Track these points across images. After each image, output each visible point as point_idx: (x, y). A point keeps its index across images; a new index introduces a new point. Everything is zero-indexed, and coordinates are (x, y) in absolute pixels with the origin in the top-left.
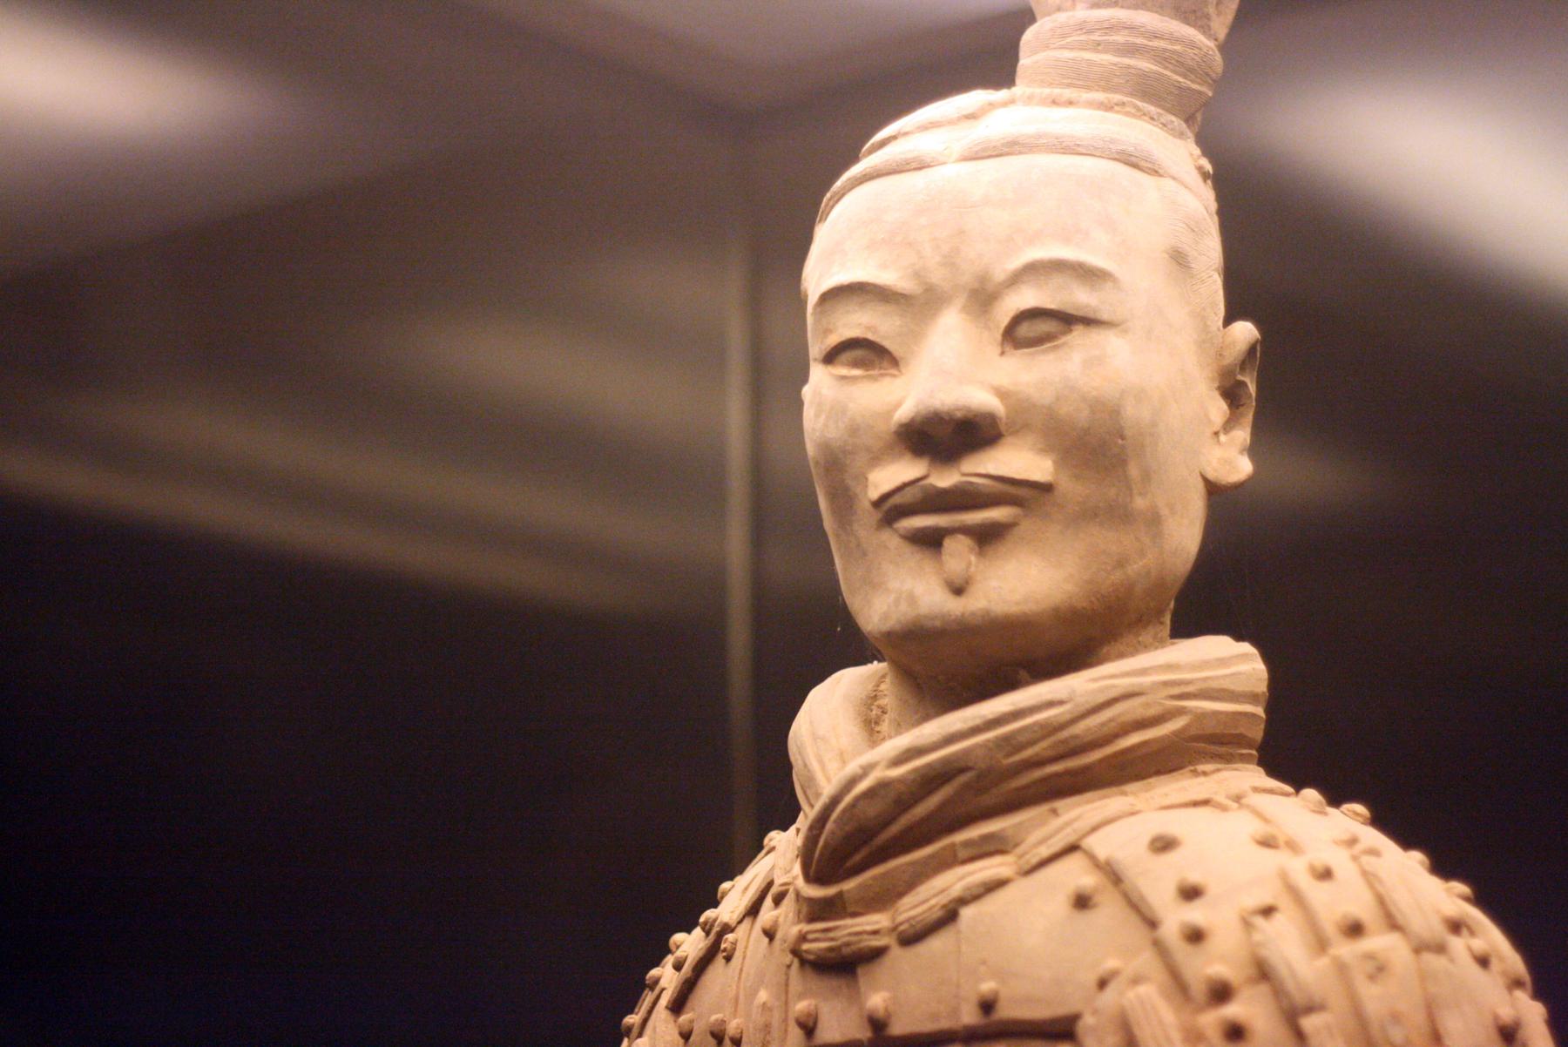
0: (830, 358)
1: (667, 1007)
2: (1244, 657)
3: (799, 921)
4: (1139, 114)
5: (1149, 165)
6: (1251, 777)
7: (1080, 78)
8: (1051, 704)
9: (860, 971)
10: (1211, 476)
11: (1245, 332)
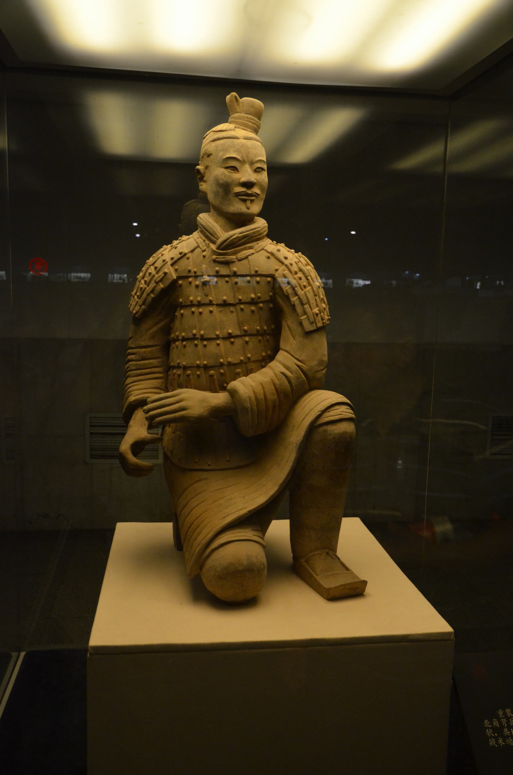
3: (213, 255)
8: (259, 228)
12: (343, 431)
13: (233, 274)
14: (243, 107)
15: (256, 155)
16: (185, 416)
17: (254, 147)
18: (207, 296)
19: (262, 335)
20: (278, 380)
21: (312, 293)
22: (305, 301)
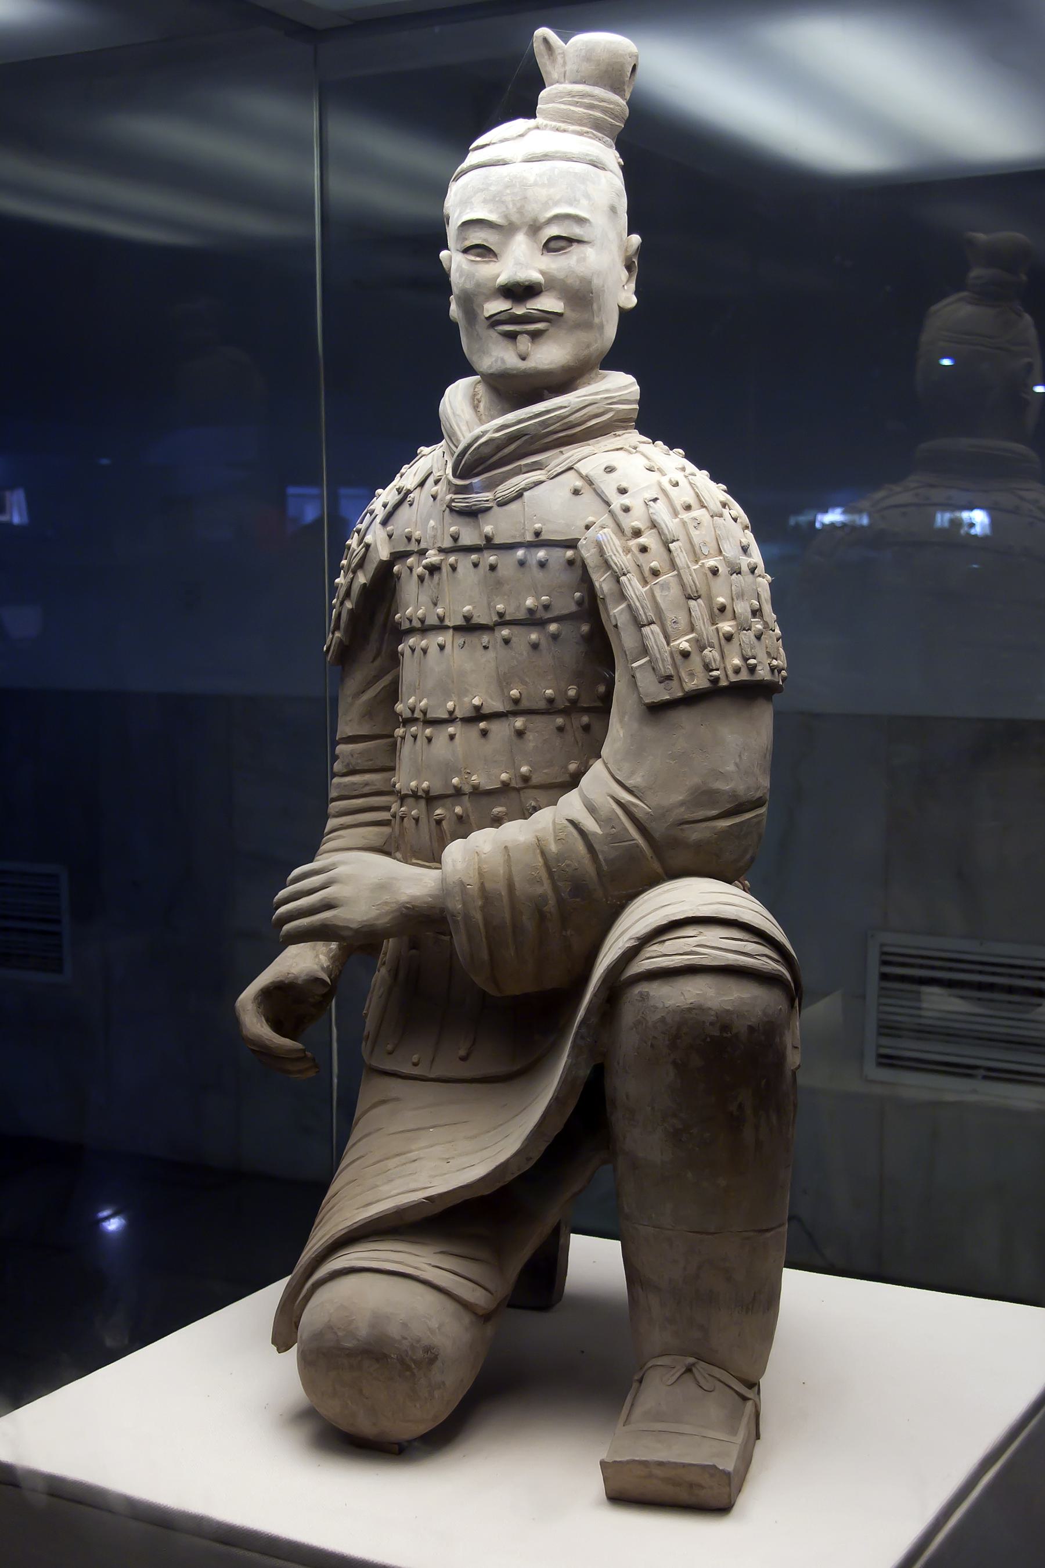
0: (466, 251)
1: (380, 523)
2: (632, 384)
3: (449, 493)
4: (596, 137)
5: (601, 166)
6: (634, 437)
7: (567, 118)
9: (479, 516)
10: (621, 305)
11: (636, 239)
12: (691, 1004)
13: (485, 543)
14: (565, 64)
15: (546, 206)
16: (329, 923)
17: (546, 182)
18: (435, 604)
19: (564, 712)
20: (558, 840)
21: (675, 591)
22: (645, 613)
